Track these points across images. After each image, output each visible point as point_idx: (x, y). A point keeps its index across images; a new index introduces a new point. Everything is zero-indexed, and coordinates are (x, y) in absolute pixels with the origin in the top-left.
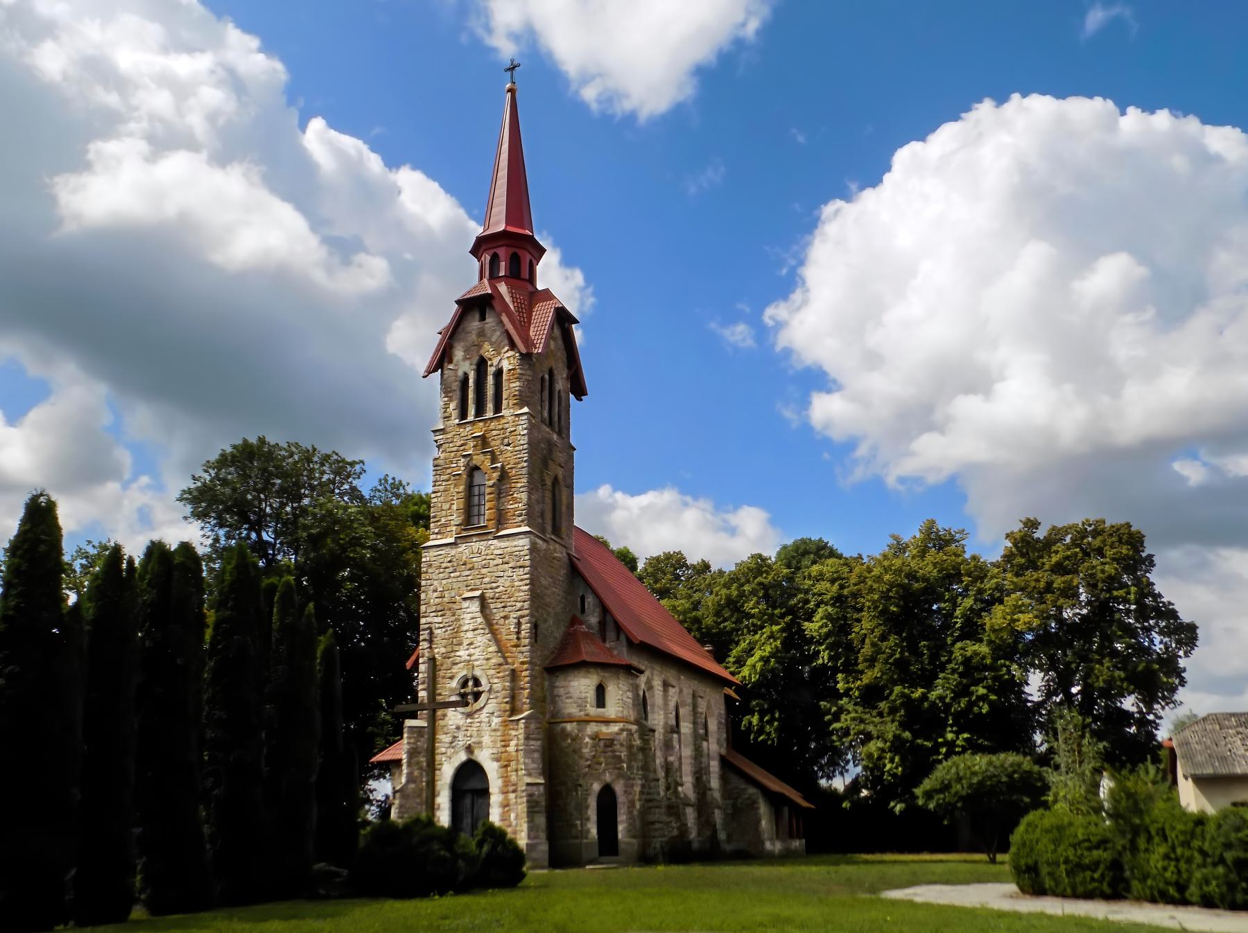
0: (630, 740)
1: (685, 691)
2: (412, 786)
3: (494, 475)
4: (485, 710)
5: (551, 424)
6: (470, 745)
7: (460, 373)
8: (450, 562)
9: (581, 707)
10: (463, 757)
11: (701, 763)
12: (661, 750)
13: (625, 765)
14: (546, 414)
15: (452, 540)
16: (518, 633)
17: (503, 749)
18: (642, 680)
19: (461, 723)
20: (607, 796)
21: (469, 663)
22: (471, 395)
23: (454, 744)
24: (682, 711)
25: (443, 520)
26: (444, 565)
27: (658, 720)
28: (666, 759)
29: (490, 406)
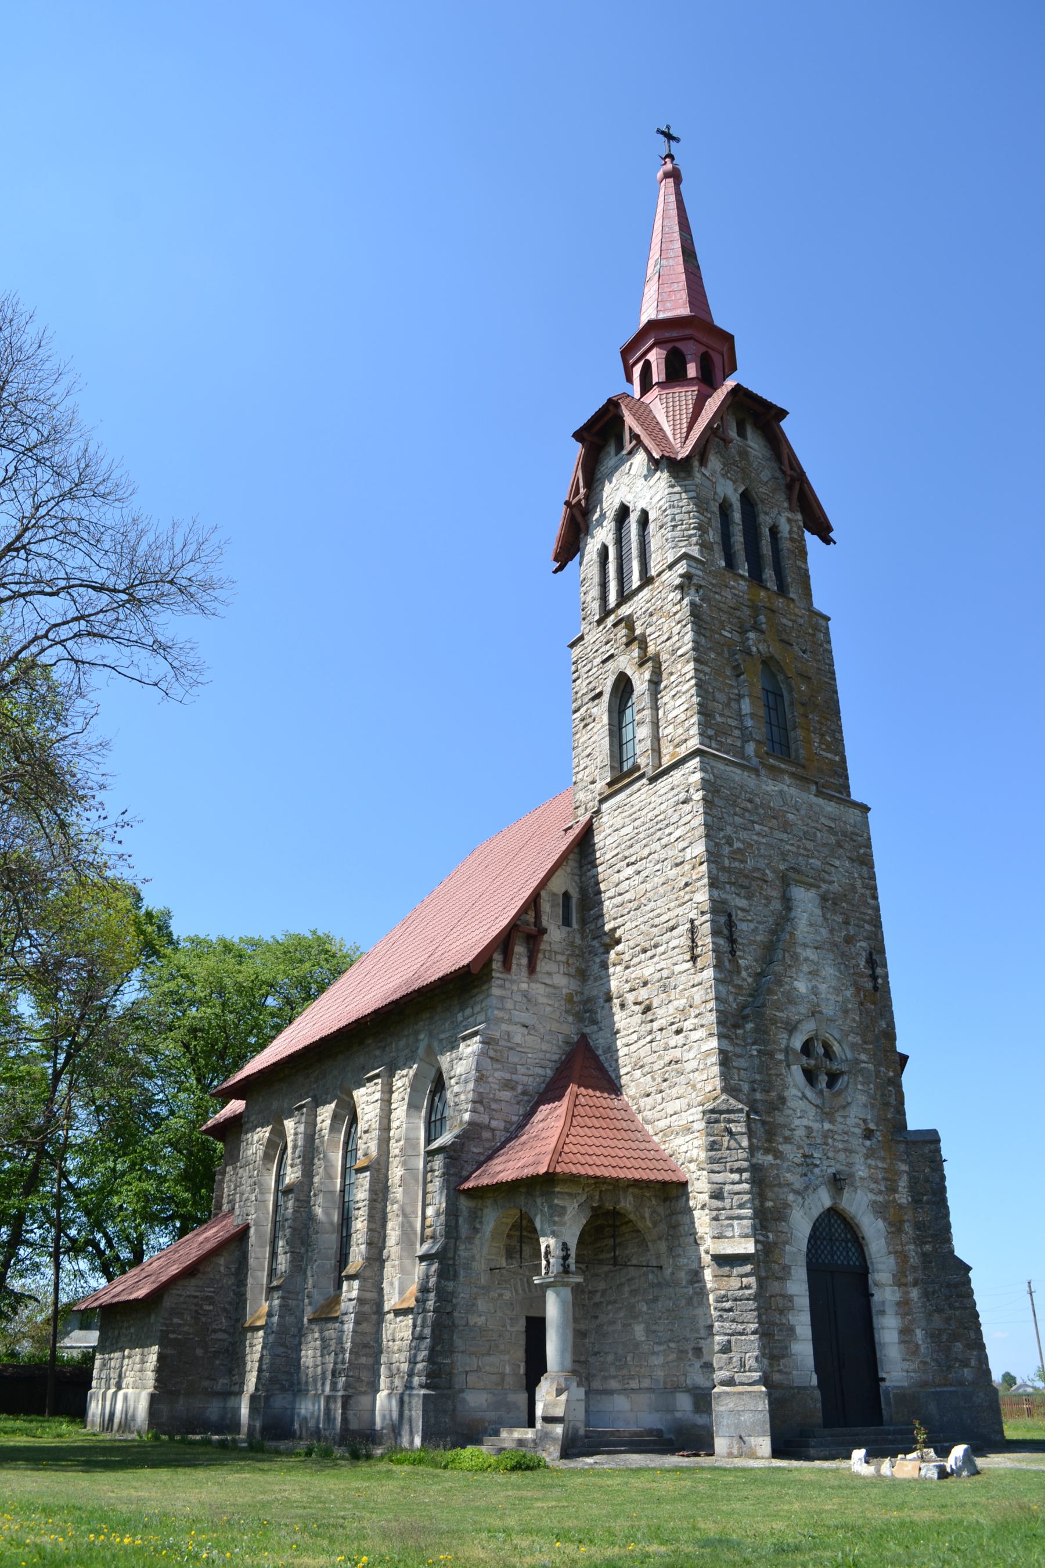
8: (750, 801)
10: (824, 1199)
19: (816, 1126)
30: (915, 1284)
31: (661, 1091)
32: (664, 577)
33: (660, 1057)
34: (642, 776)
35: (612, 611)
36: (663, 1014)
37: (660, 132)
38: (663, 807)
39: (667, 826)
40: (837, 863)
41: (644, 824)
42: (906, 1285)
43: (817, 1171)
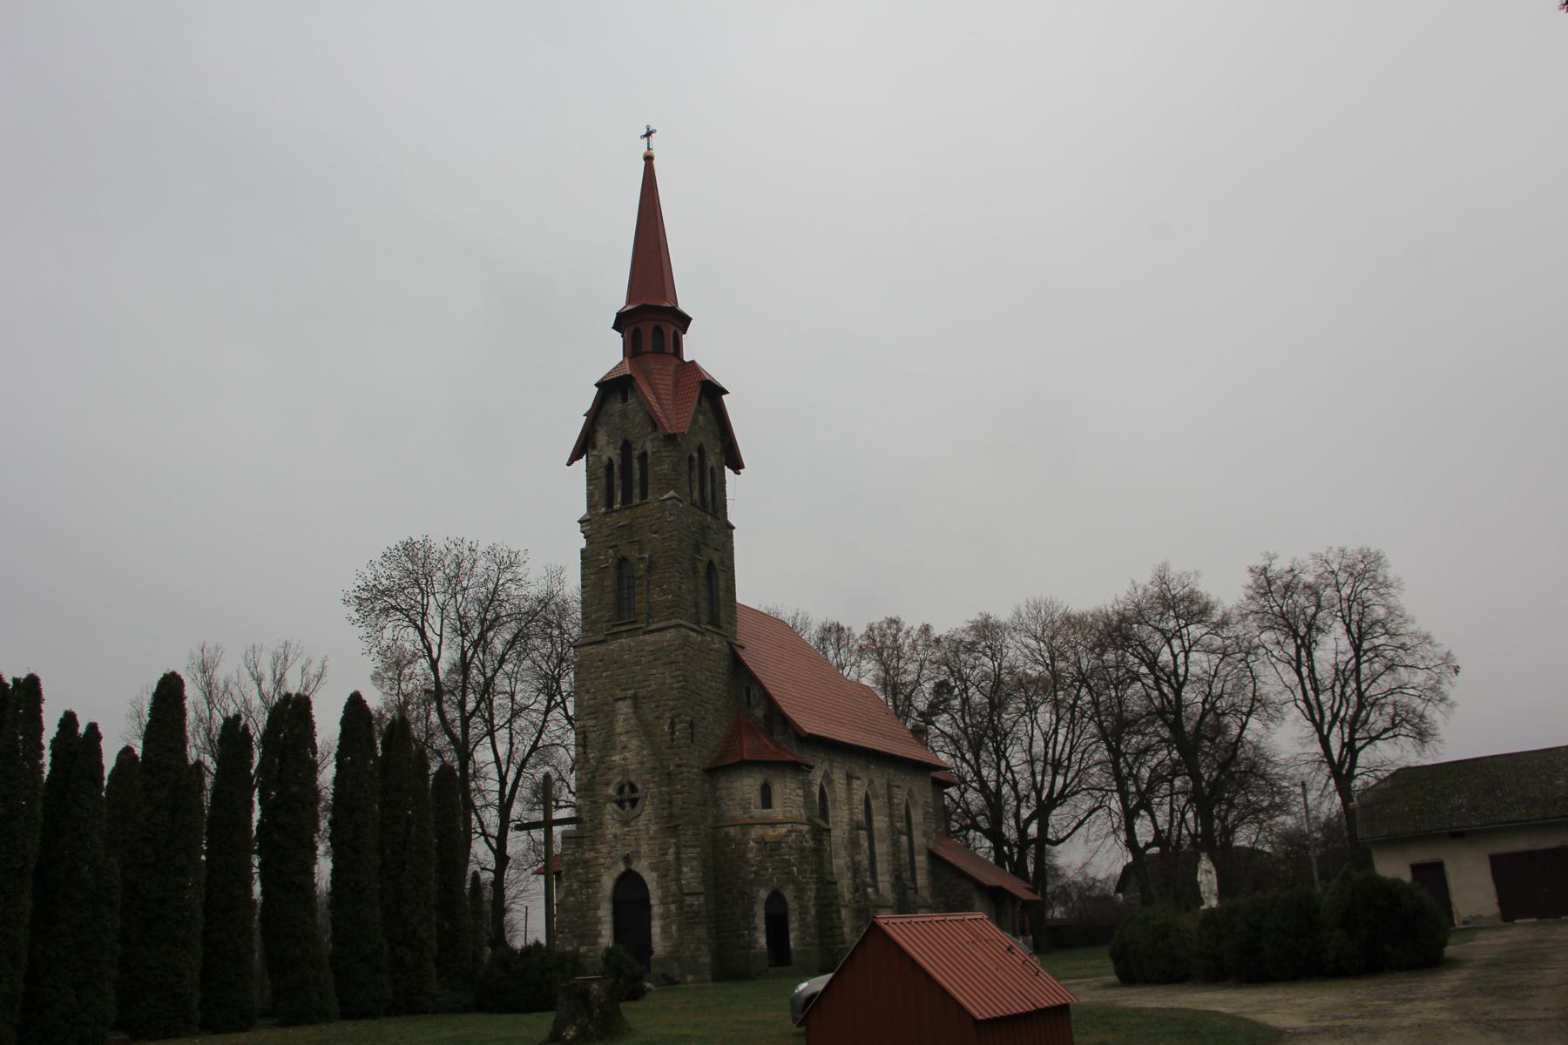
0: (801, 842)
1: (877, 782)
2: (572, 899)
3: (642, 566)
4: (642, 818)
5: (703, 505)
6: (628, 854)
7: (605, 459)
8: (601, 660)
9: (745, 809)
10: (622, 868)
11: (899, 859)
12: (846, 849)
13: (795, 869)
14: (696, 495)
15: (600, 638)
16: (672, 733)
17: (662, 859)
18: (817, 776)
19: (618, 832)
20: (776, 898)
21: (625, 772)
22: (617, 482)
23: (612, 854)
24: (873, 804)
25: (593, 616)
26: (596, 665)
27: (841, 819)
28: (853, 859)
29: (637, 491)
30: (673, 902)
40: (654, 671)
42: (666, 904)
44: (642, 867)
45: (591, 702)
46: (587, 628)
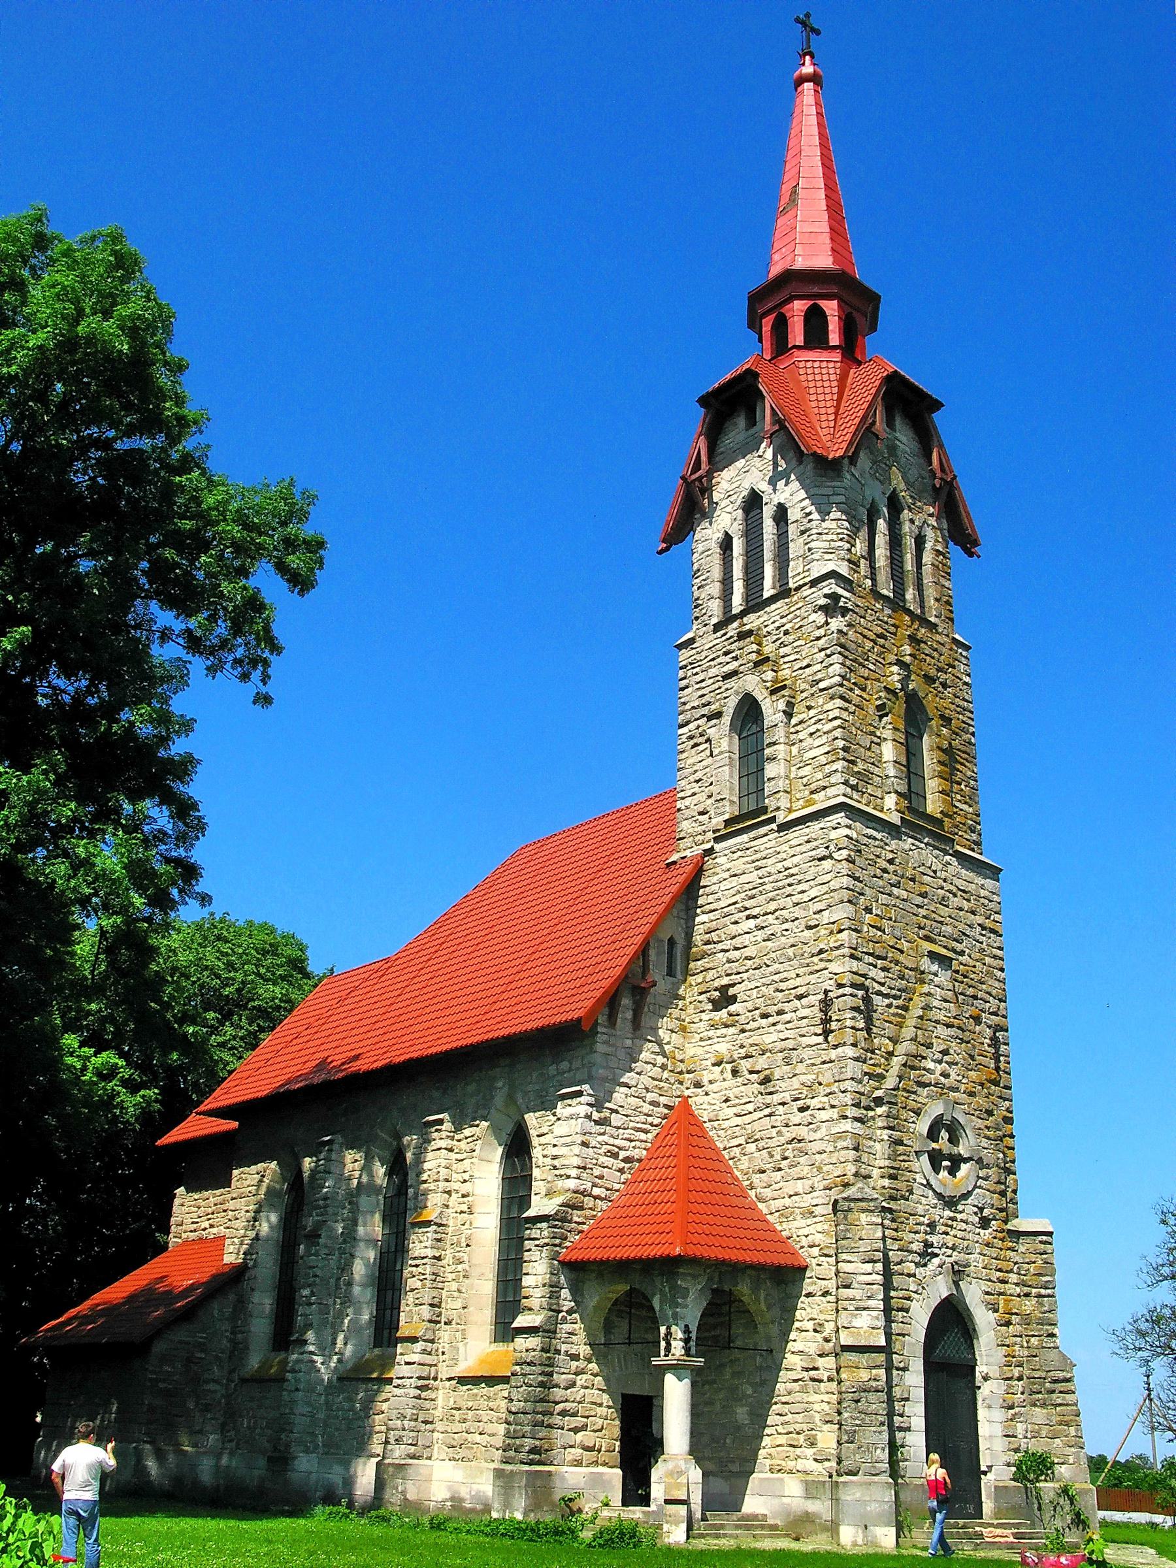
10: (942, 1289)
31: (780, 1169)
32: (806, 591)
33: (779, 1133)
34: (773, 820)
35: (734, 618)
36: (786, 1088)
37: (797, 20)
38: (796, 860)
39: (800, 882)
41: (770, 874)
43: (936, 1261)
44: (974, 1295)
45: (873, 931)
46: (853, 781)
